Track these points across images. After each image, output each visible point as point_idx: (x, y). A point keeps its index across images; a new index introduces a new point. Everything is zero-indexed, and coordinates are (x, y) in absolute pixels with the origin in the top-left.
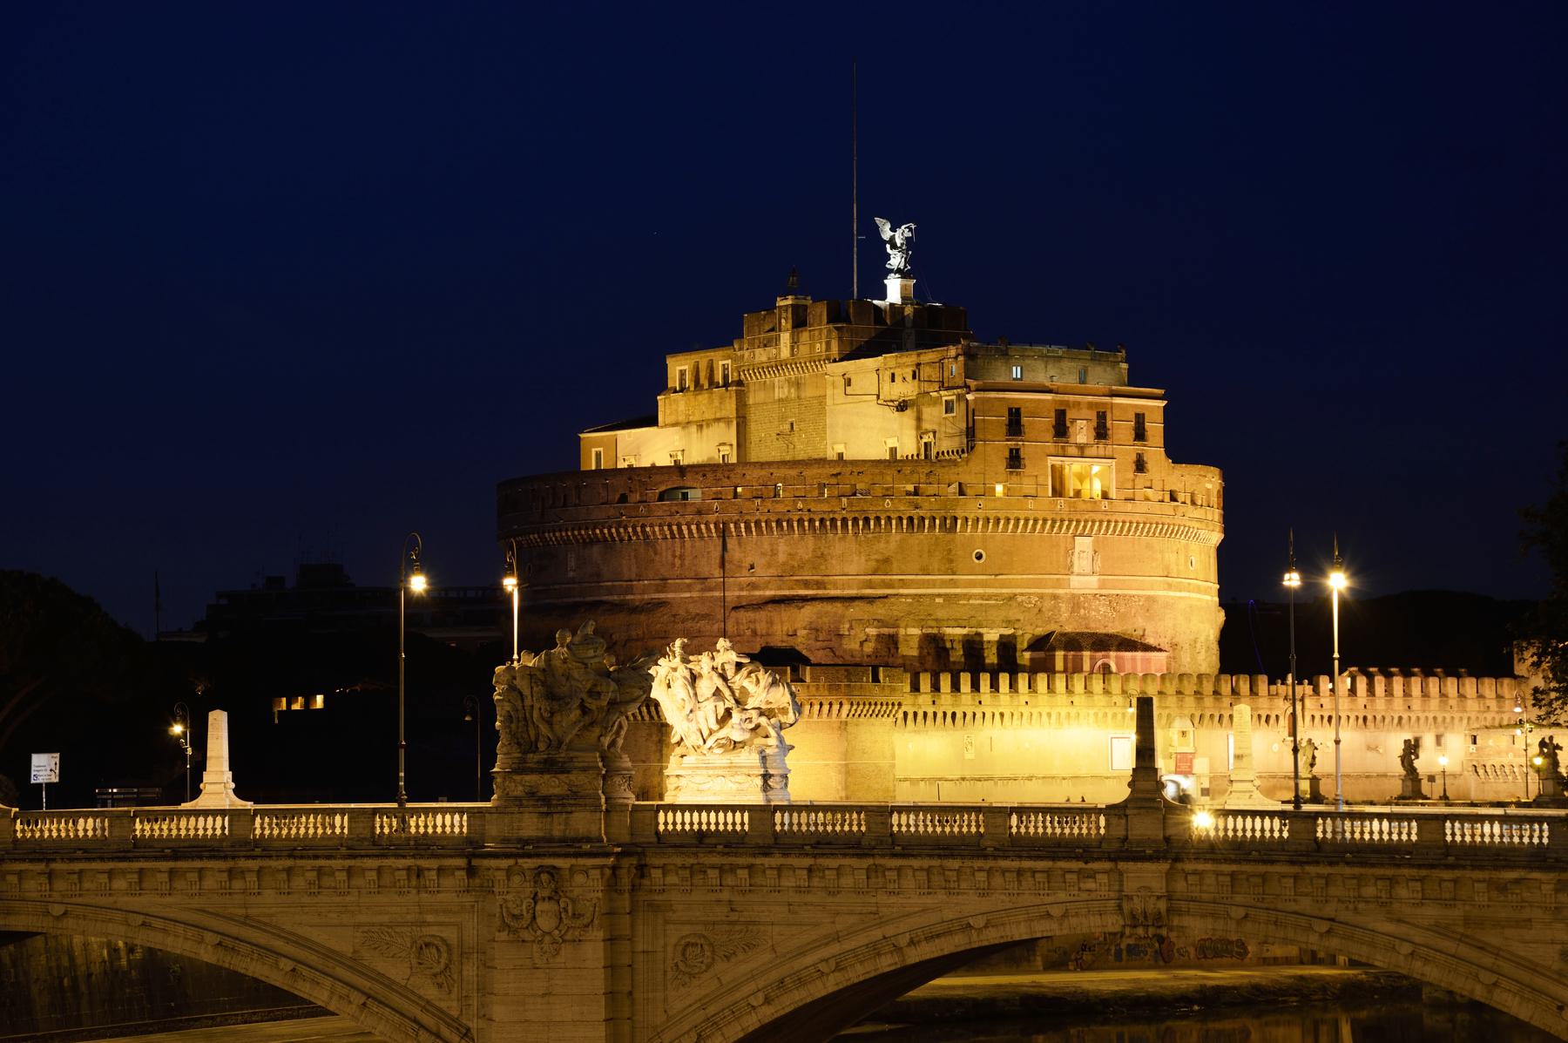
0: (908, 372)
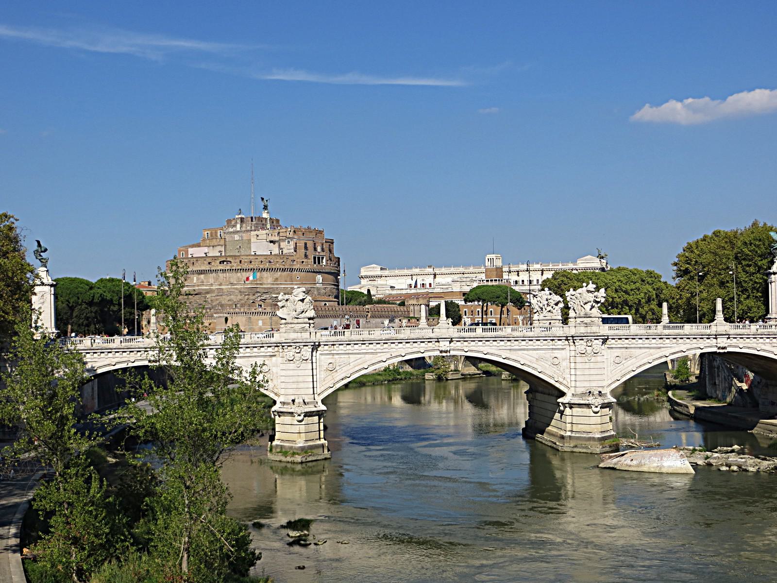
0: (276, 234)
